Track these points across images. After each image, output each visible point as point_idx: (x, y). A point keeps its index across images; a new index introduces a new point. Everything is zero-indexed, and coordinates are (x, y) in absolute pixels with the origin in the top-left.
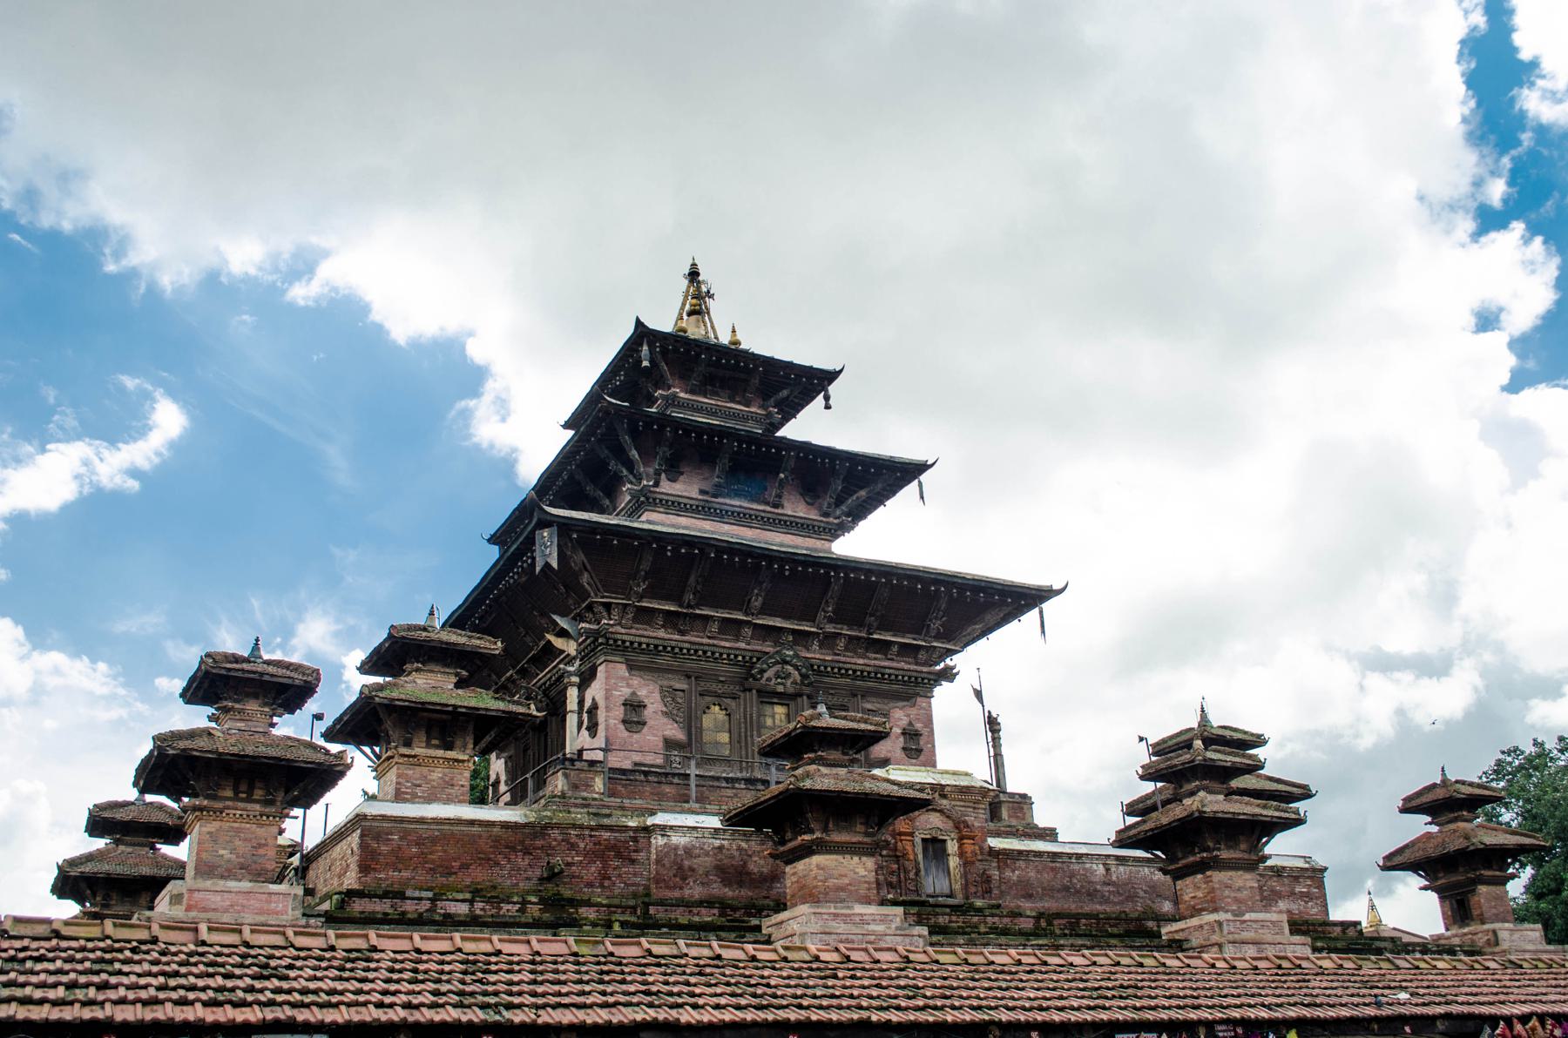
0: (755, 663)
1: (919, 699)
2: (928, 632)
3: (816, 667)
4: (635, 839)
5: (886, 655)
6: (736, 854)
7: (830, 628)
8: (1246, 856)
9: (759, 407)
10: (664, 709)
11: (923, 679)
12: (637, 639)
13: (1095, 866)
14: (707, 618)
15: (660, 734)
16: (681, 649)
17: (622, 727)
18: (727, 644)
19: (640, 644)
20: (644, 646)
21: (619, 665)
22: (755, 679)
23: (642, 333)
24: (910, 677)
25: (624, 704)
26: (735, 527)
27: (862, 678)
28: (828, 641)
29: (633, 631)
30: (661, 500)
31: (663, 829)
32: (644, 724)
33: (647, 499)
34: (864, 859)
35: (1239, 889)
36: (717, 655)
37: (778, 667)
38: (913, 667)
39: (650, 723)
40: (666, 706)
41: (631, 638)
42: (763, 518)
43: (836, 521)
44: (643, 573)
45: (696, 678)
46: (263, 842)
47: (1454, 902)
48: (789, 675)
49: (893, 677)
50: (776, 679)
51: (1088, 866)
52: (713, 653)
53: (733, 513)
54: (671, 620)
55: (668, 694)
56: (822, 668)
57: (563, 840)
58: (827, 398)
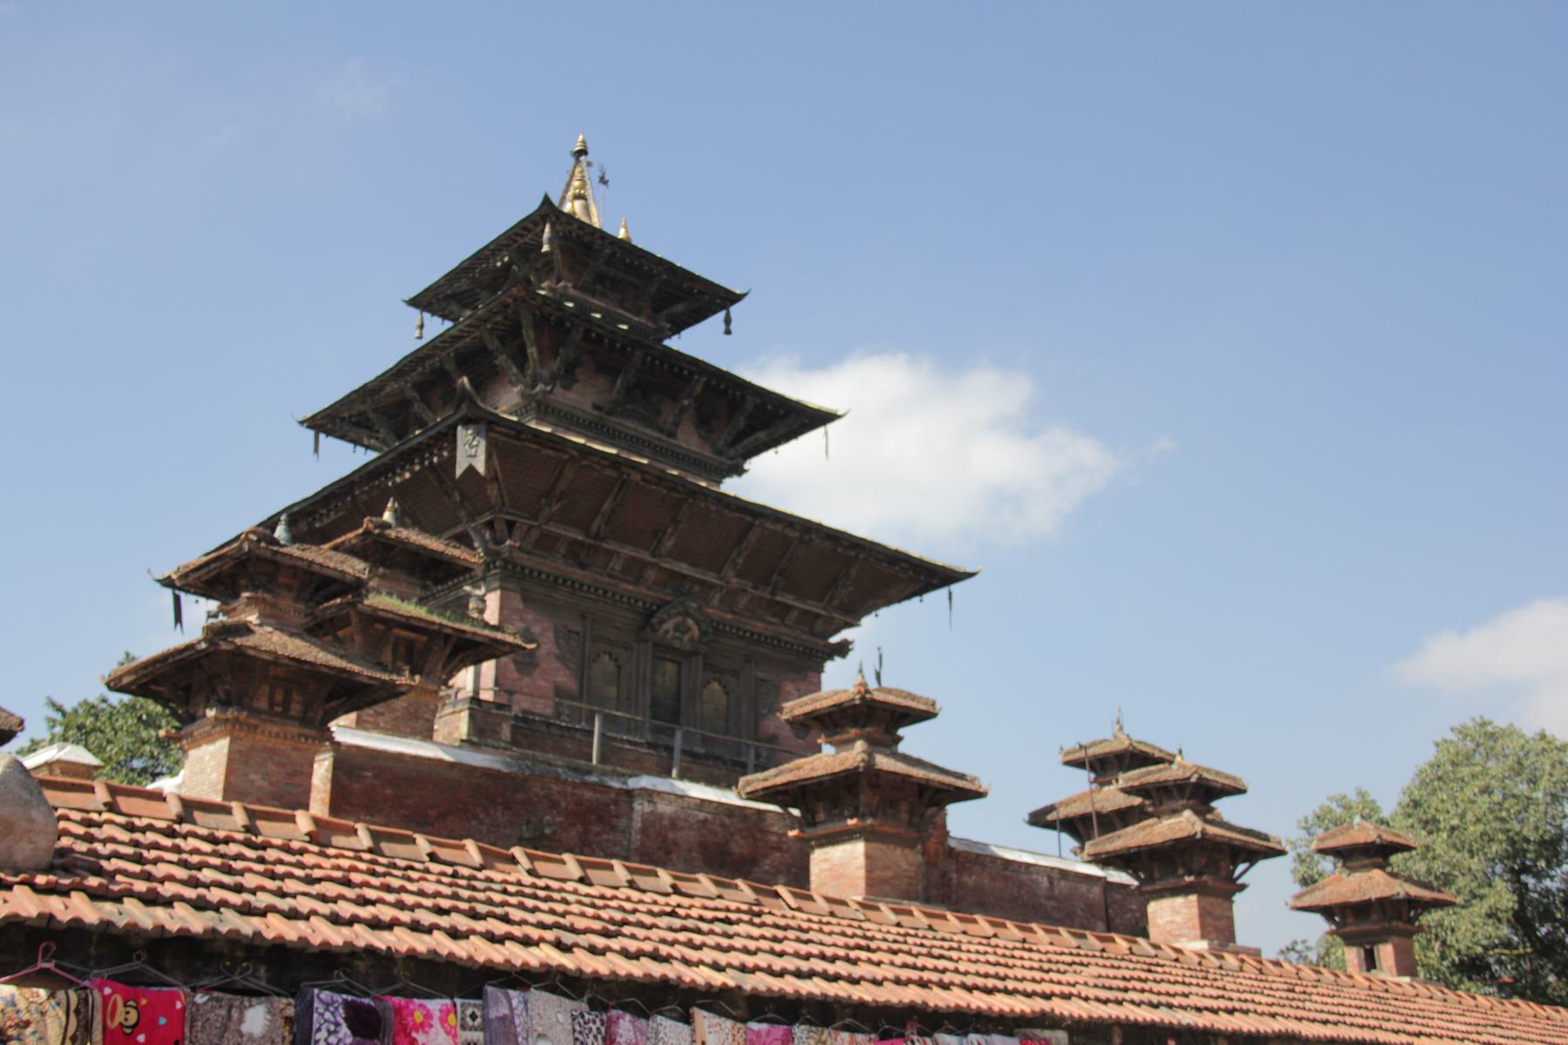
0: (651, 614)
1: (811, 674)
2: (831, 601)
4: (616, 803)
5: (783, 621)
6: (719, 829)
7: (735, 582)
9: (649, 319)
10: (557, 652)
11: (818, 651)
13: (1040, 878)
14: (610, 553)
19: (540, 573)
20: (543, 576)
21: (513, 594)
23: (548, 211)
24: (805, 648)
31: (650, 795)
32: (536, 666)
34: (907, 851)
35: (1219, 918)
36: (617, 597)
37: (679, 619)
40: (558, 646)
42: (656, 446)
43: (729, 462)
46: (298, 768)
47: (1362, 951)
48: (689, 629)
49: (789, 646)
51: (1034, 877)
52: (614, 595)
53: (626, 435)
54: (576, 553)
55: (563, 635)
57: (544, 796)
58: (728, 321)
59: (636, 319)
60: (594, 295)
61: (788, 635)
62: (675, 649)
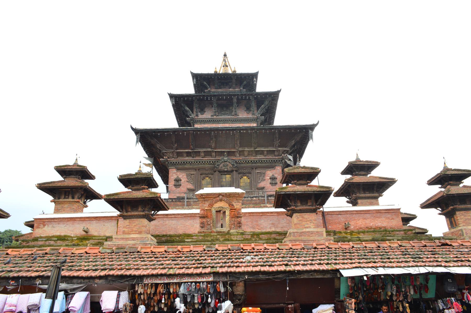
1: (276, 167)
3: (237, 162)
8: (311, 207)
10: (187, 180)
11: (277, 161)
12: (177, 161)
14: (199, 152)
15: (186, 187)
16: (192, 162)
17: (174, 187)
18: (206, 159)
19: (179, 162)
20: (180, 163)
22: (217, 168)
24: (272, 161)
25: (174, 180)
26: (223, 124)
27: (255, 163)
28: (241, 153)
29: (178, 159)
30: (198, 121)
33: (194, 121)
36: (204, 162)
38: (274, 157)
39: (182, 185)
40: (188, 179)
41: (176, 161)
42: (231, 120)
44: (174, 142)
45: (198, 170)
49: (265, 161)
50: (224, 166)
52: (202, 162)
53: (221, 120)
54: (188, 154)
56: (240, 162)
59: (234, 90)
60: (221, 89)
61: (264, 159)
62: (226, 171)
